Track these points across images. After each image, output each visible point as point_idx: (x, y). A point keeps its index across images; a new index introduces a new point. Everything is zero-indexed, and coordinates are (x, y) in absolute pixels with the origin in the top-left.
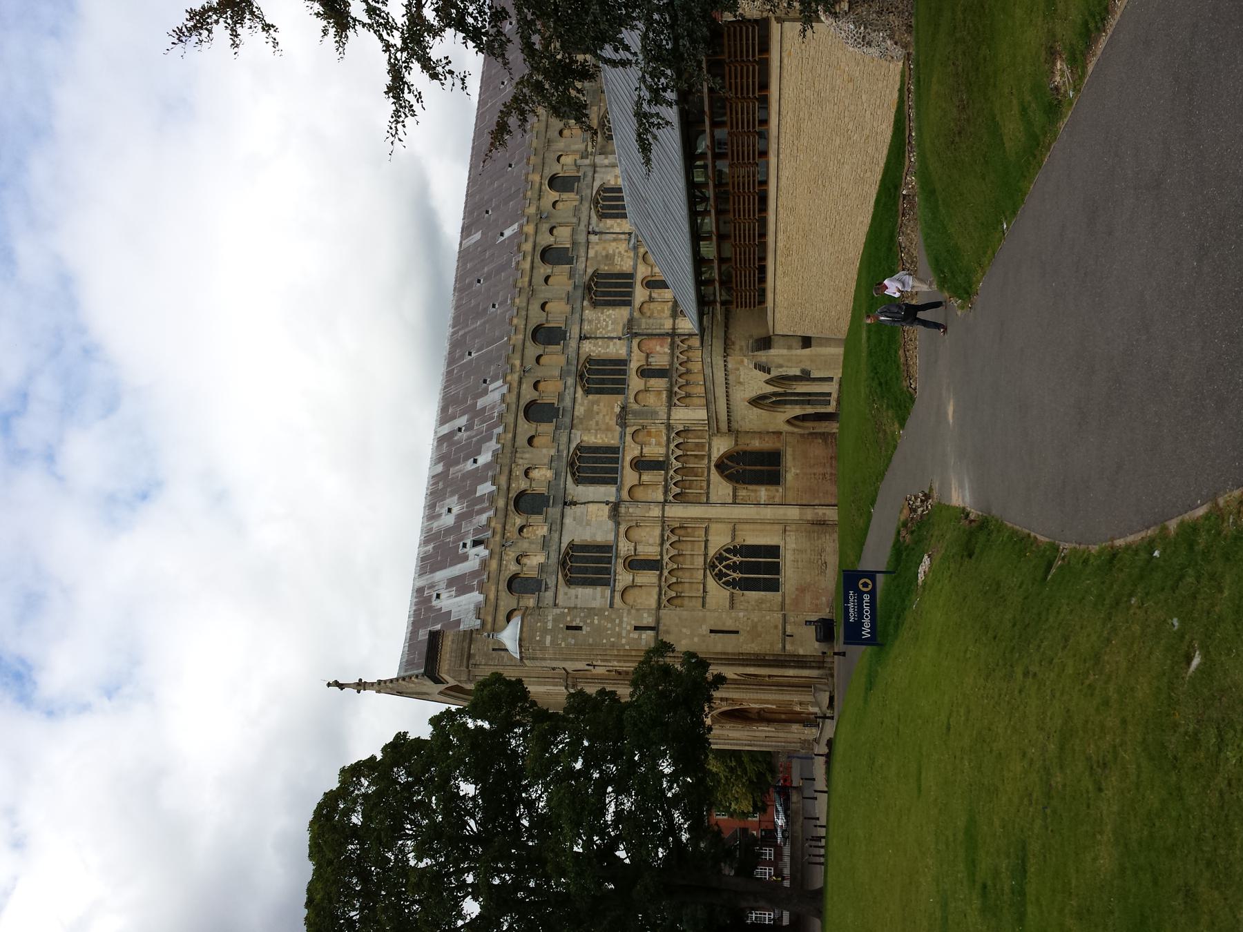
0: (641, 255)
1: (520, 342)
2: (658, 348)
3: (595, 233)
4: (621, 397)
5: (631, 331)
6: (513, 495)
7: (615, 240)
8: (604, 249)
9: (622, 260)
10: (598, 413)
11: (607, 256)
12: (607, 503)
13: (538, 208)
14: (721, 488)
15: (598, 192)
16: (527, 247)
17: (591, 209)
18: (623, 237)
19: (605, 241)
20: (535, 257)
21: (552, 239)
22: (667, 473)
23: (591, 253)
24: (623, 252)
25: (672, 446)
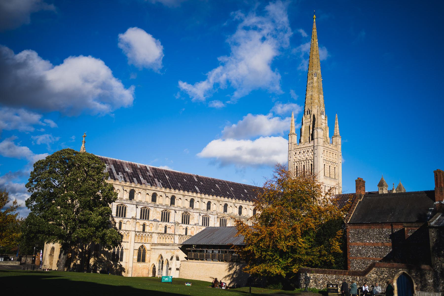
0: (194, 226)
1: (172, 192)
2: (172, 230)
4: (160, 220)
5: (176, 224)
6: (135, 189)
7: (197, 220)
10: (157, 214)
11: (193, 218)
12: (136, 216)
14: (138, 246)
18: (198, 222)
21: (196, 202)
22: (142, 232)
23: (195, 214)
25: (148, 234)
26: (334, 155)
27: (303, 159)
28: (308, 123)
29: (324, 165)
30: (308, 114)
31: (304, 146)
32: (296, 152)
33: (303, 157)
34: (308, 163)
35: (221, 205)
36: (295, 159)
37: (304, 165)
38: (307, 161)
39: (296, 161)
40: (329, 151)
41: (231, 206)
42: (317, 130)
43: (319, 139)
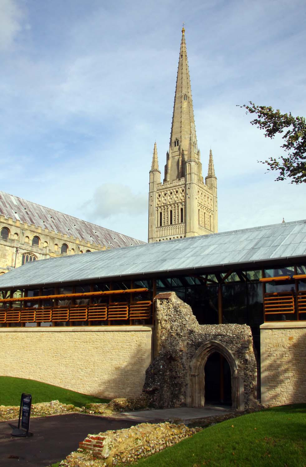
3: (17, 251)
7: (12, 260)
8: (9, 254)
9: (3, 262)
11: (5, 255)
13: (27, 229)
15: (34, 255)
16: (10, 222)
17: (27, 251)
18: (14, 264)
19: (13, 255)
20: (5, 224)
23: (7, 248)
24: (6, 263)
26: (209, 199)
27: (169, 202)
28: (176, 157)
29: (199, 210)
30: (175, 146)
31: (172, 185)
32: (160, 193)
33: (170, 200)
34: (176, 208)
35: (56, 245)
36: (159, 203)
37: (171, 211)
38: (176, 205)
39: (160, 205)
40: (204, 194)
41: (73, 249)
42: (190, 162)
43: (193, 175)
